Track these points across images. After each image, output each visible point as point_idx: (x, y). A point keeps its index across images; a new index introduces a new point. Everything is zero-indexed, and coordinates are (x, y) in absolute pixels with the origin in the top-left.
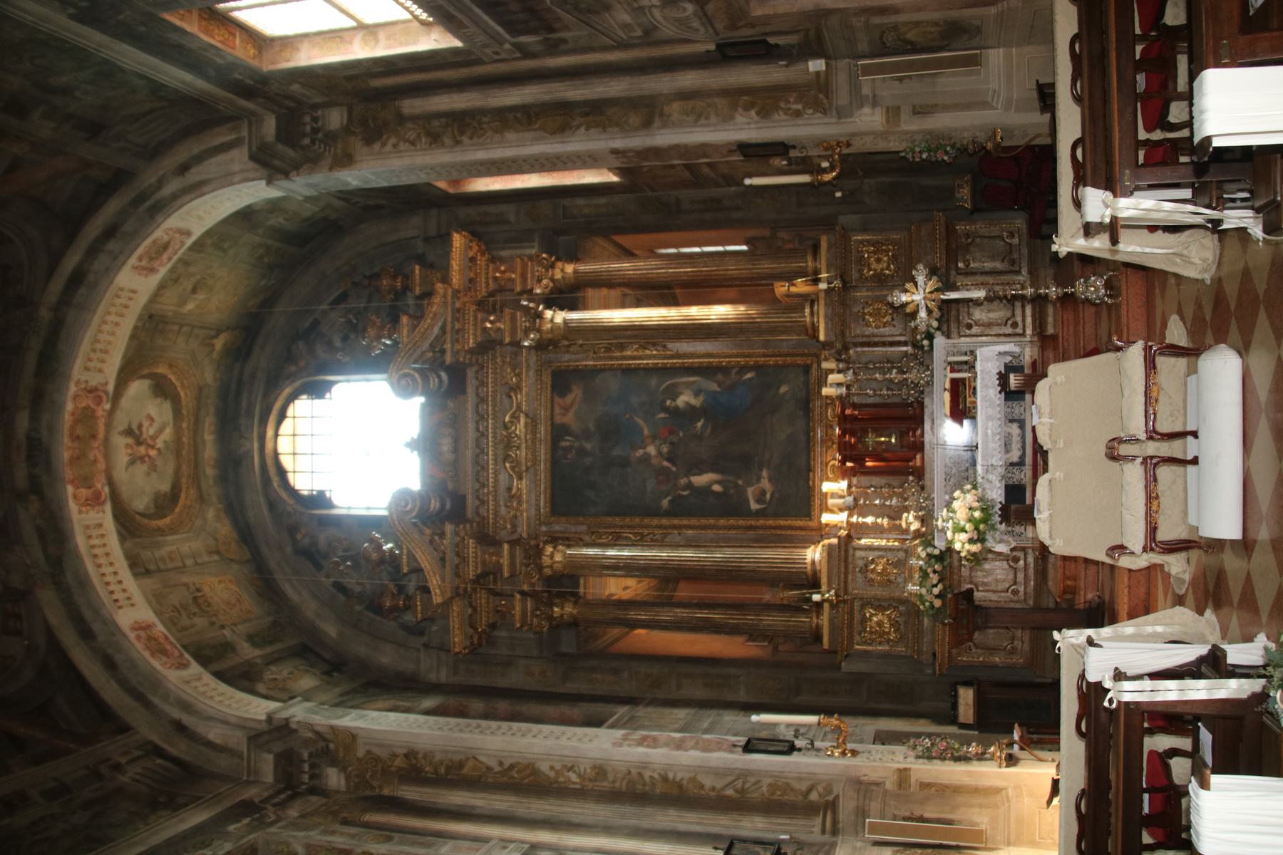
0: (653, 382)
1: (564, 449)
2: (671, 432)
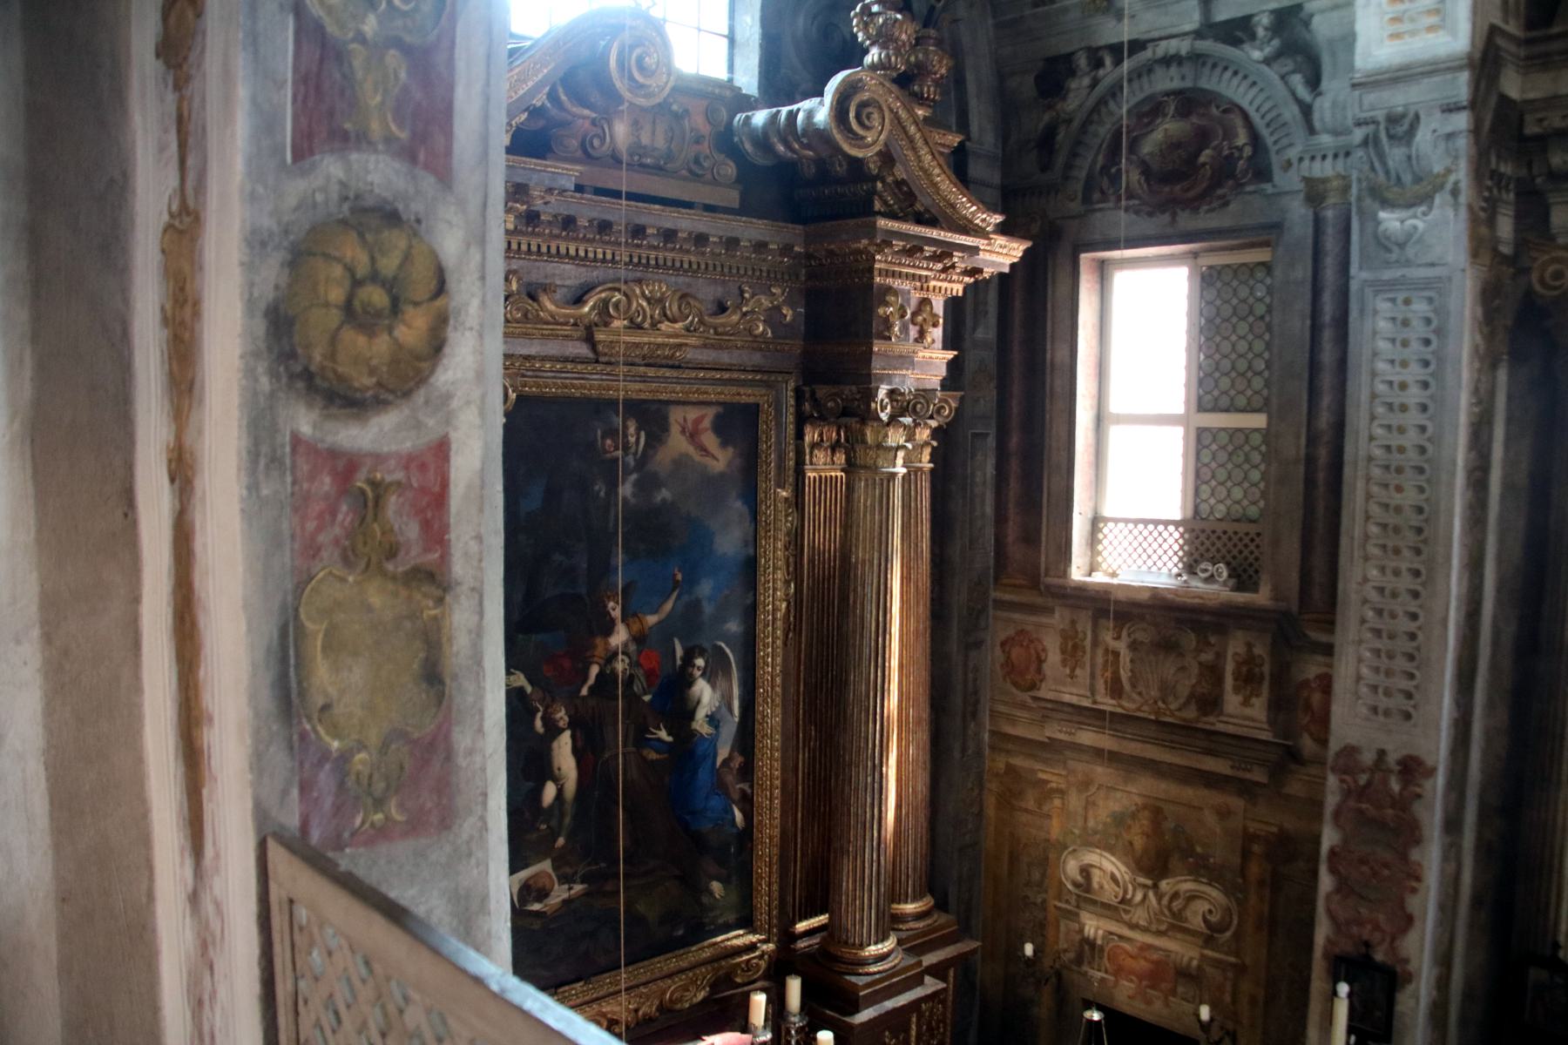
0: (734, 626)
2: (650, 674)
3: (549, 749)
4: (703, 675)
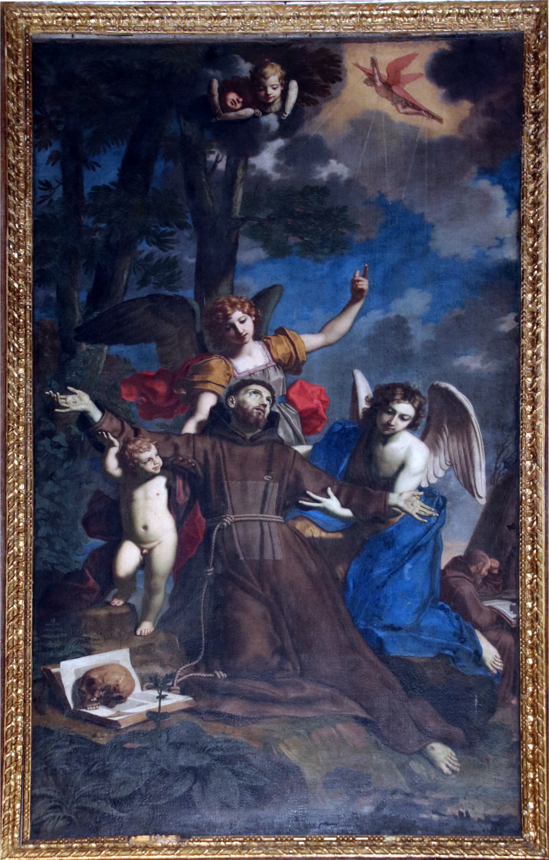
1: (257, 81)
2: (309, 420)
3: (131, 500)
4: (412, 427)
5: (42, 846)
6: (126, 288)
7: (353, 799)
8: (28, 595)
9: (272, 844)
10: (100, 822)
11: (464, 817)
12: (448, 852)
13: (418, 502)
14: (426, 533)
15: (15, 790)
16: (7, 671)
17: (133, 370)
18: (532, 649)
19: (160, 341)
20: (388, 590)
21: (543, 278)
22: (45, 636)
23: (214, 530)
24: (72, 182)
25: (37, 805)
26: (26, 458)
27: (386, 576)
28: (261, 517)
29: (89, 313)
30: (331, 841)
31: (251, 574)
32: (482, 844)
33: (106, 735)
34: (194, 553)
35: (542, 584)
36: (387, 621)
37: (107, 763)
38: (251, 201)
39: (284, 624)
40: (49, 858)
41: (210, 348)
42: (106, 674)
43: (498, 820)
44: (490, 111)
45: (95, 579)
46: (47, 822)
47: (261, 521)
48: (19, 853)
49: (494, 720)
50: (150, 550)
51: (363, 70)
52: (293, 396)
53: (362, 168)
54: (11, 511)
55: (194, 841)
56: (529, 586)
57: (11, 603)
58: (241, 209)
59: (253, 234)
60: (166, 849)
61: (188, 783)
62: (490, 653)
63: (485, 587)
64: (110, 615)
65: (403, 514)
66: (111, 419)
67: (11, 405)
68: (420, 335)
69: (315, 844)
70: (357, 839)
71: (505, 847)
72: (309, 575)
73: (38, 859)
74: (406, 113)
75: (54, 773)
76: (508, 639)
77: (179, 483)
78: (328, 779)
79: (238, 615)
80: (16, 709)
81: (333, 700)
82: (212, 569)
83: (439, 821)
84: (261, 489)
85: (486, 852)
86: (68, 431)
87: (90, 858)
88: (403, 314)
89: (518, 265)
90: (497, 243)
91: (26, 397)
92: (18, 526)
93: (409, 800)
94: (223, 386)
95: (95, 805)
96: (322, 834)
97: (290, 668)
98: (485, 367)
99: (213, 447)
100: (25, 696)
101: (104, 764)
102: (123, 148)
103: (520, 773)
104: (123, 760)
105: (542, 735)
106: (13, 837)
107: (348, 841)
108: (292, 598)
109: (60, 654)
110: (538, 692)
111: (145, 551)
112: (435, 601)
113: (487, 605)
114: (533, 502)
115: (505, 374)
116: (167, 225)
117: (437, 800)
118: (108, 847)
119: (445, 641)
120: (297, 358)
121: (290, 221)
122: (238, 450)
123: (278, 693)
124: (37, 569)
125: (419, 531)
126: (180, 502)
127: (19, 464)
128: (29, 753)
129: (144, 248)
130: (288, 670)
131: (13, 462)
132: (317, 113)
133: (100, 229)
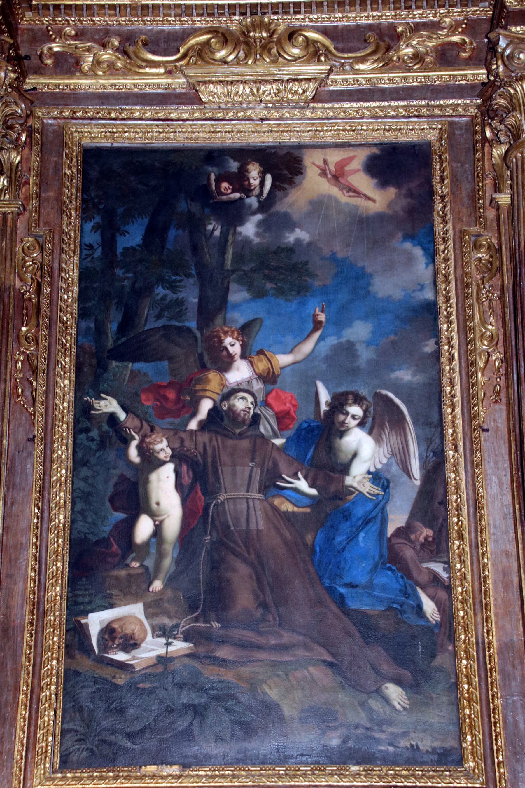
2: (283, 419)
3: (147, 481)
4: (361, 425)
5: (69, 775)
6: (146, 320)
7: (324, 733)
8: (65, 558)
9: (258, 773)
10: (116, 753)
11: (415, 749)
12: (403, 780)
13: (368, 483)
14: (375, 508)
15: (48, 725)
16: (46, 622)
17: (151, 381)
18: (462, 603)
19: (171, 359)
20: (347, 554)
21: (455, 313)
22: (78, 592)
23: (210, 505)
24: (108, 244)
25: (66, 738)
26: (67, 449)
27: (345, 542)
28: (247, 495)
29: (118, 339)
30: (307, 770)
31: (240, 541)
32: (431, 773)
33: (123, 676)
34: (195, 524)
35: (467, 549)
36: (347, 579)
37: (124, 701)
38: (239, 258)
39: (265, 582)
40: (74, 786)
41: (208, 365)
42: (124, 624)
43: (442, 751)
44: (410, 194)
45: (118, 545)
46: (73, 753)
47: (247, 499)
48: (50, 781)
49: (436, 664)
50: (161, 522)
51: (318, 167)
52: (270, 401)
53: (319, 234)
54: (54, 490)
55: (193, 770)
56: (457, 551)
57: (51, 565)
58: (232, 263)
59: (240, 281)
60: (170, 778)
61: (189, 718)
62: (429, 607)
63: (422, 551)
64: (129, 575)
65: (357, 492)
66: (133, 418)
67: (58, 408)
68: (365, 355)
69: (293, 773)
70: (327, 768)
71: (450, 776)
72: (285, 543)
73: (65, 787)
74: (350, 196)
75: (80, 709)
76: (442, 595)
77: (184, 468)
78: (302, 714)
79: (229, 575)
80: (52, 655)
81: (306, 647)
82: (209, 537)
83: (395, 752)
84: (247, 473)
85: (434, 781)
86: (100, 428)
87: (108, 786)
88: (352, 340)
89: (435, 303)
90: (419, 287)
91: (69, 402)
92: (60, 503)
93: (369, 733)
94: (218, 394)
95: (113, 738)
96: (299, 764)
97: (271, 619)
98: (415, 379)
99: (211, 441)
100: (59, 643)
101: (121, 702)
102: (146, 221)
103: (458, 709)
104: (137, 699)
105: (475, 676)
106: (45, 767)
107: (320, 770)
108: (272, 561)
109: (89, 608)
110: (469, 639)
111: (157, 523)
112: (384, 563)
113: (425, 566)
114: (456, 483)
115: (430, 384)
116: (177, 274)
117: (392, 734)
118: (123, 776)
119: (393, 597)
120: (274, 372)
121: (267, 272)
122: (230, 442)
123: (262, 640)
124: (73, 537)
125: (370, 506)
126: (185, 484)
127: (62, 454)
128: (61, 692)
129: (160, 291)
130: (269, 621)
131: (57, 452)
132: (286, 196)
133: (128, 278)
